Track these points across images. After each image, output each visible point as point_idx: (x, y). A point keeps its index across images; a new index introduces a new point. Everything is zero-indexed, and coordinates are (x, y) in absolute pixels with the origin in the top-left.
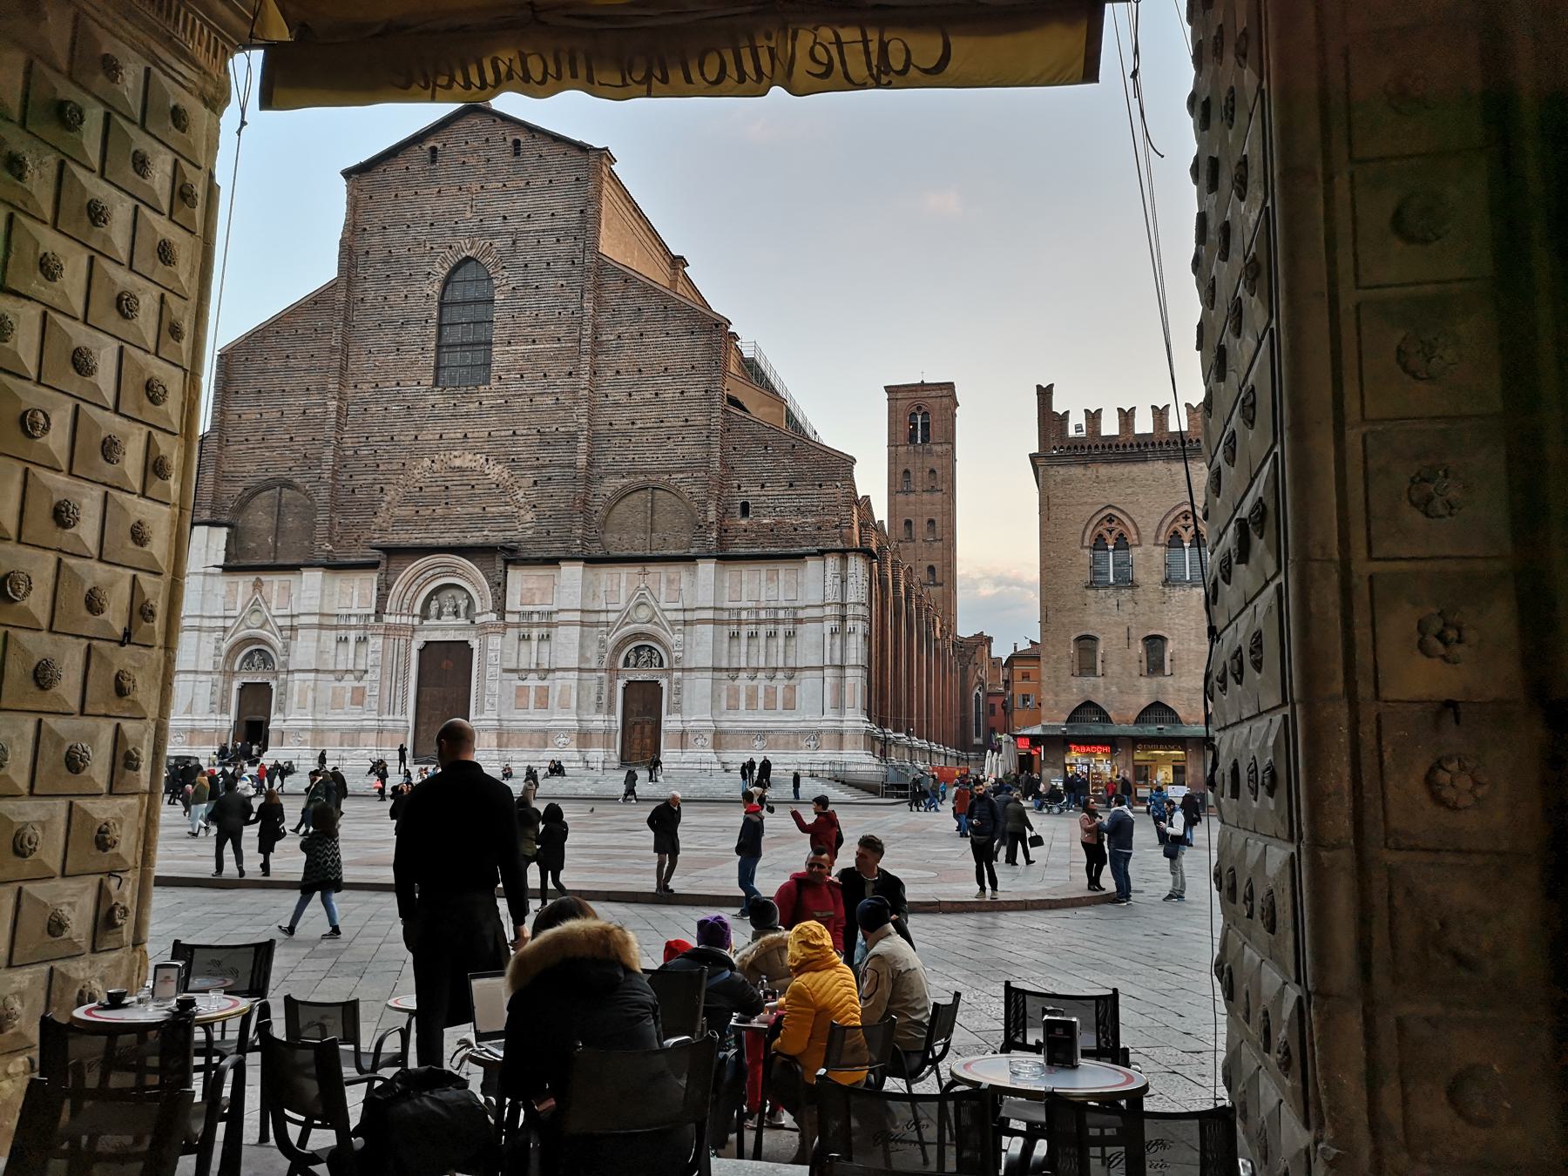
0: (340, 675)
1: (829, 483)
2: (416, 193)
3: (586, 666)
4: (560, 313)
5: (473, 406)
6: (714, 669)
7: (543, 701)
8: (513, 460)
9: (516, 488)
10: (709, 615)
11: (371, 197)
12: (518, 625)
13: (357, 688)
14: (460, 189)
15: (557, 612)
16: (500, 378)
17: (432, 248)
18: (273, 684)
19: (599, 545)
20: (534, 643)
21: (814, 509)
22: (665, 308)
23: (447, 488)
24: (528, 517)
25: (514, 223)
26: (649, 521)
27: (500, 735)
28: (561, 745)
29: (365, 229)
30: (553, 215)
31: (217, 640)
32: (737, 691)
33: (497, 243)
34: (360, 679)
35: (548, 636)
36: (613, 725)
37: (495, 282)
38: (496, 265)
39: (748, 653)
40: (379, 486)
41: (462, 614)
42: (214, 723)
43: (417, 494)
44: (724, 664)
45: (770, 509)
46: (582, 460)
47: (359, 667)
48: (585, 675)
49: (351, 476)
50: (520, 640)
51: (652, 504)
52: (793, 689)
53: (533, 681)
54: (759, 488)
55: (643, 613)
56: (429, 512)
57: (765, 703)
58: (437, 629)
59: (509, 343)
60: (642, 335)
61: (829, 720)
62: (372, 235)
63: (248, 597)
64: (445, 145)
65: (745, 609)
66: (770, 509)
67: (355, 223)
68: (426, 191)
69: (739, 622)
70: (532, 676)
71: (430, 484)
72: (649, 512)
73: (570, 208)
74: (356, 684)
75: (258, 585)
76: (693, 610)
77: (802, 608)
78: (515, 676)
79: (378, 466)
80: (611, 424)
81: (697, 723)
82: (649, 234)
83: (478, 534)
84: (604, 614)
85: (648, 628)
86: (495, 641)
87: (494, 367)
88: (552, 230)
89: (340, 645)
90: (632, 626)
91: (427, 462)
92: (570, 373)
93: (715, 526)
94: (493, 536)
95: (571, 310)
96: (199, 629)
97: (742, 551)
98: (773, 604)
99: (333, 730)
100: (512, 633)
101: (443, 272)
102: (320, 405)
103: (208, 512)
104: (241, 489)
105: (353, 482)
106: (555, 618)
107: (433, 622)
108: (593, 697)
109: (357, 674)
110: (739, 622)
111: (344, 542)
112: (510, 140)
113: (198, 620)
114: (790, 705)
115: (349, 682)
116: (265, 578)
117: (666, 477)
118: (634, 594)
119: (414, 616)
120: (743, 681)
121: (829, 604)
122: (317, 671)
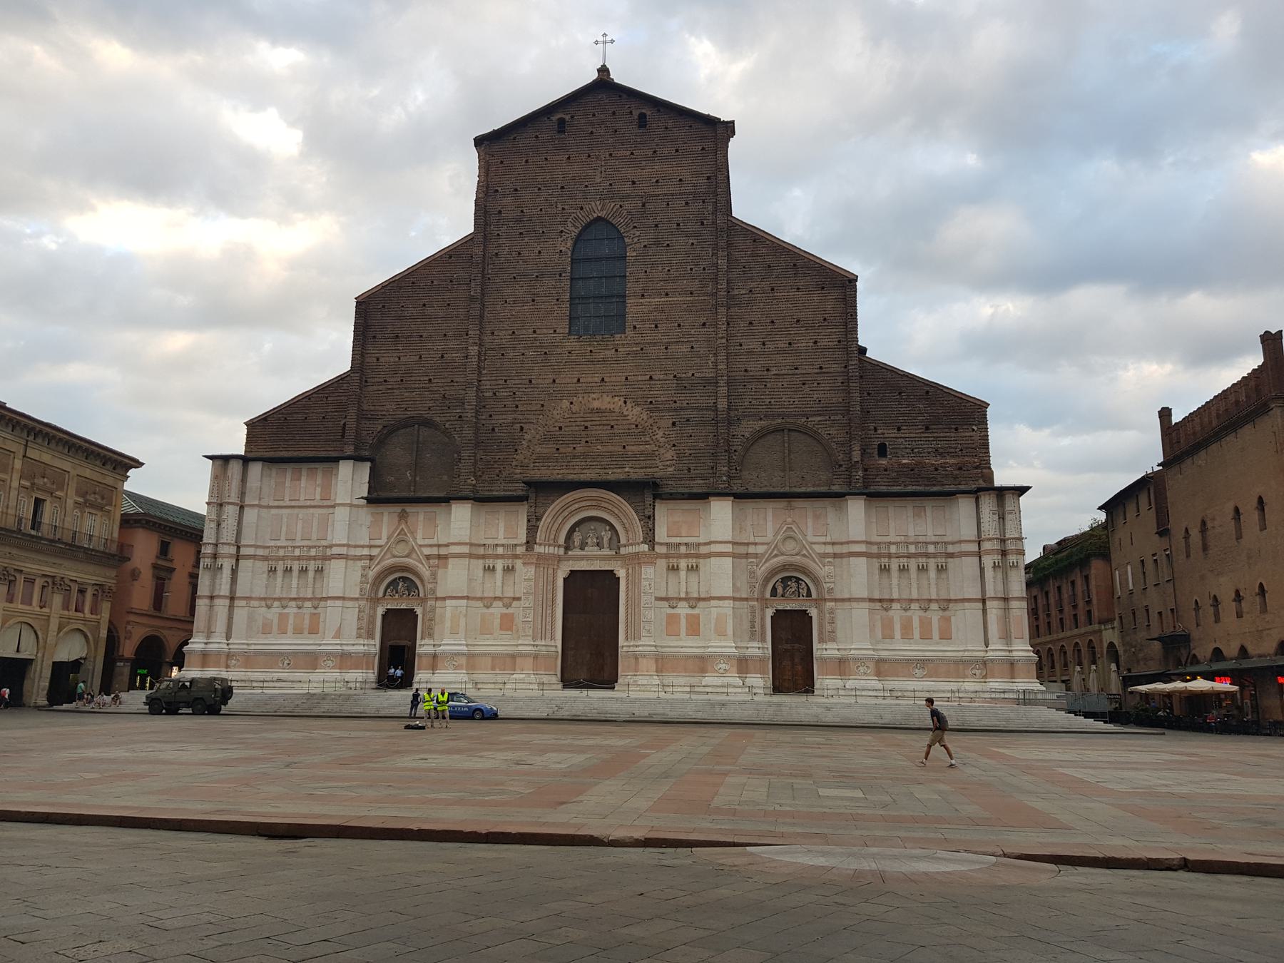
0: (488, 602)
1: (965, 427)
4: (691, 269)
6: (871, 600)
7: (694, 629)
8: (651, 402)
9: (655, 428)
10: (862, 548)
11: (502, 162)
12: (667, 556)
13: (506, 614)
14: (589, 156)
15: (709, 543)
16: (635, 327)
17: (563, 209)
18: (419, 611)
19: (740, 481)
21: (953, 450)
22: (795, 265)
23: (586, 427)
24: (669, 455)
26: (787, 460)
27: (657, 660)
28: (721, 671)
29: (497, 191)
30: (681, 180)
31: (364, 568)
32: (891, 620)
33: (627, 205)
34: (507, 606)
35: (697, 566)
36: (766, 652)
37: (626, 240)
38: (627, 224)
39: (899, 585)
40: (519, 425)
42: (362, 647)
43: (558, 433)
44: (877, 596)
45: (908, 451)
46: (722, 404)
47: (507, 595)
48: (737, 603)
49: (491, 416)
51: (789, 444)
52: (948, 620)
53: (683, 610)
54: (895, 431)
55: (790, 546)
56: (570, 450)
57: (921, 633)
58: (582, 559)
59: (643, 295)
60: (773, 289)
61: (997, 649)
63: (394, 527)
64: (572, 117)
65: (893, 543)
66: (908, 451)
67: (487, 187)
69: (890, 556)
71: (569, 424)
72: (787, 451)
74: (505, 611)
75: (403, 516)
76: (842, 544)
77: (953, 543)
78: (666, 604)
79: (517, 407)
80: (746, 371)
81: (857, 652)
83: (619, 470)
84: (754, 546)
85: (798, 559)
86: (648, 572)
87: (629, 317)
88: (680, 194)
90: (781, 558)
91: (565, 404)
92: (704, 324)
93: (860, 465)
95: (702, 268)
97: (884, 489)
98: (921, 539)
99: (484, 655)
100: (662, 563)
102: (458, 350)
103: (352, 448)
104: (380, 427)
105: (493, 422)
106: (703, 550)
107: (577, 552)
108: (746, 625)
109: (506, 601)
110: (890, 556)
111: (485, 477)
112: (636, 113)
113: (345, 548)
114: (946, 635)
115: (497, 609)
116: (410, 509)
117: (804, 420)
118: (780, 528)
119: (559, 546)
120: (896, 613)
121: (990, 540)
122: (467, 598)
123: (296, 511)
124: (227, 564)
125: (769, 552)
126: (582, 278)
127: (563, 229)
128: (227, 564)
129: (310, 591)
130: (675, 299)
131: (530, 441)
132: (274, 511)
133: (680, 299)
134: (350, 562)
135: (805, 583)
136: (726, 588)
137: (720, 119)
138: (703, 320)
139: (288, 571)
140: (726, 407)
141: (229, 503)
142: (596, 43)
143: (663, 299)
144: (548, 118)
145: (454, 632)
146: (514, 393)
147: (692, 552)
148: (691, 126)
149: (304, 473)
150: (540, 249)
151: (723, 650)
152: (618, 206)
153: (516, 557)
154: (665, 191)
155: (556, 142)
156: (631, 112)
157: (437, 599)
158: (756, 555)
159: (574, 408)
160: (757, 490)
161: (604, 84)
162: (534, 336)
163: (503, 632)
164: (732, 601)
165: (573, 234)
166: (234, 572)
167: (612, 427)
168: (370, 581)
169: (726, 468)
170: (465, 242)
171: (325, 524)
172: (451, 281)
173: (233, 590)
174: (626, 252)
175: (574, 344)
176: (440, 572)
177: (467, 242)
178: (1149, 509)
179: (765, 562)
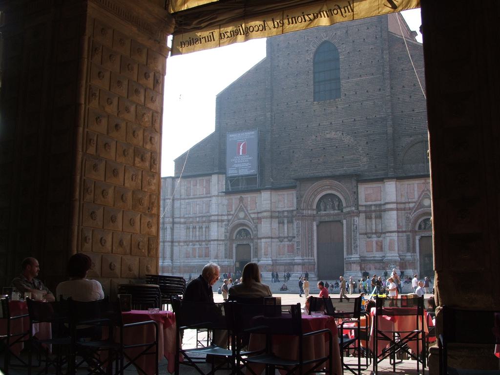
0: (281, 239)
3: (401, 230)
4: (372, 62)
5: (334, 109)
12: (365, 212)
16: (345, 95)
17: (308, 39)
20: (374, 221)
23: (324, 148)
24: (365, 160)
33: (339, 33)
37: (339, 50)
40: (292, 150)
41: (336, 208)
46: (390, 130)
48: (400, 234)
50: (366, 218)
53: (374, 239)
59: (349, 78)
70: (374, 236)
75: (241, 200)
78: (366, 236)
79: (291, 141)
80: (402, 112)
82: (402, 21)
87: (342, 90)
88: (364, 24)
89: (281, 225)
92: (380, 90)
94: (350, 170)
96: (218, 221)
100: (362, 216)
108: (405, 245)
119: (313, 210)
122: (272, 238)
123: (196, 200)
124: (168, 226)
125: (416, 206)
127: (307, 49)
128: (168, 226)
129: (204, 237)
131: (297, 158)
132: (187, 201)
133: (367, 77)
134: (220, 223)
138: (378, 87)
139: (194, 228)
140: (392, 132)
141: (167, 199)
145: (266, 255)
146: (289, 134)
147: (378, 209)
149: (198, 182)
151: (393, 258)
152: (334, 34)
153: (293, 216)
157: (258, 239)
158: (410, 209)
159: (318, 139)
160: (411, 174)
163: (289, 254)
164: (397, 234)
166: (172, 229)
167: (337, 147)
169: (392, 164)
171: (209, 205)
173: (172, 238)
174: (339, 56)
176: (259, 225)
177: (264, 62)
179: (414, 212)
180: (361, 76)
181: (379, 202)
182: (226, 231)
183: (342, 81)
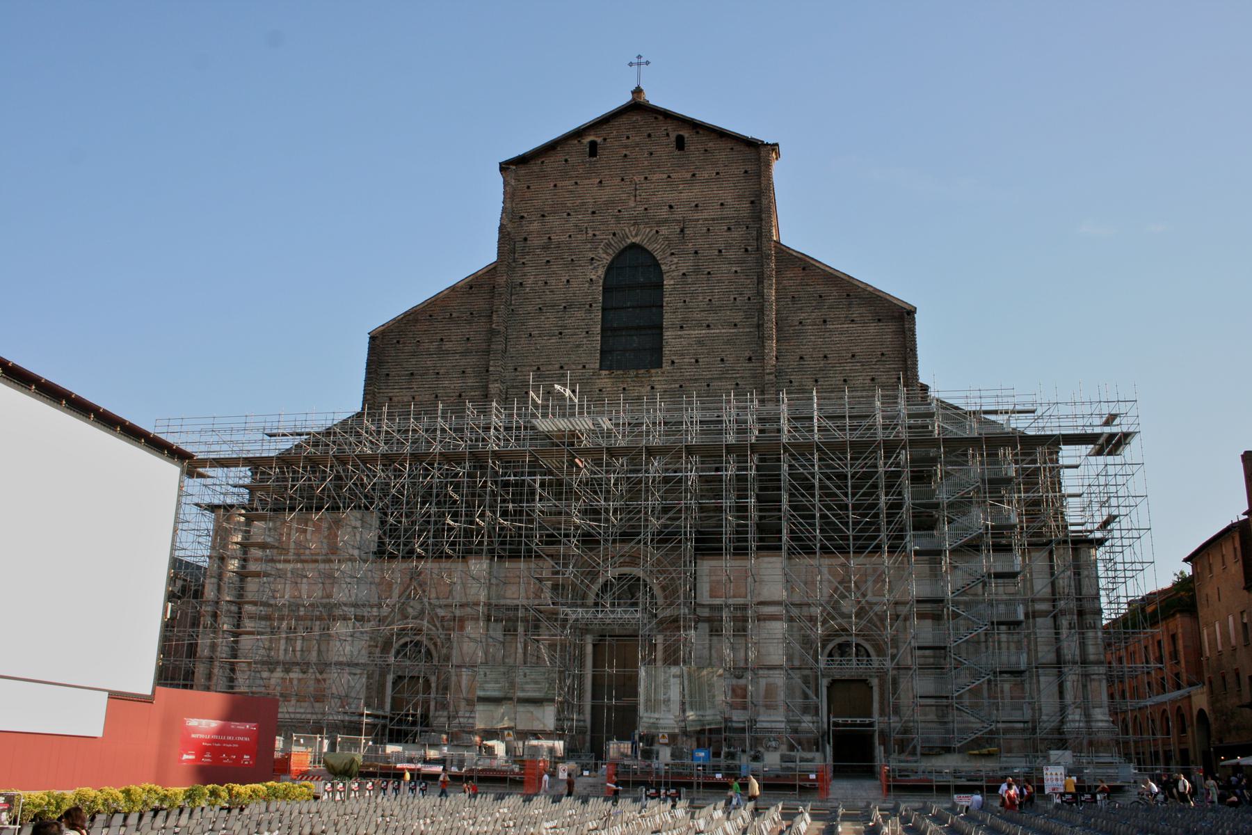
2: (576, 183)
4: (735, 299)
11: (528, 187)
14: (623, 180)
16: (673, 362)
17: (594, 235)
25: (679, 213)
29: (522, 217)
30: (722, 204)
33: (664, 231)
37: (663, 267)
38: (663, 251)
59: (682, 327)
60: (825, 321)
62: (531, 222)
64: (605, 139)
68: (587, 182)
73: (740, 198)
81: (923, 724)
87: (666, 350)
88: (721, 219)
92: (750, 359)
95: (747, 296)
101: (608, 257)
112: (673, 136)
126: (615, 309)
127: (593, 256)
129: (314, 654)
130: (718, 331)
133: (723, 331)
135: (865, 648)
136: (776, 655)
137: (763, 142)
138: (747, 354)
142: (631, 64)
143: (704, 332)
144: (579, 141)
148: (732, 149)
150: (568, 278)
151: (774, 725)
154: (705, 215)
155: (587, 166)
156: (668, 135)
161: (637, 107)
162: (562, 372)
165: (605, 261)
168: (379, 645)
170: (487, 272)
172: (471, 314)
175: (606, 380)
177: (491, 271)
178: (1236, 562)
180: (708, 326)
181: (741, 601)
182: (372, 643)
183: (668, 334)
